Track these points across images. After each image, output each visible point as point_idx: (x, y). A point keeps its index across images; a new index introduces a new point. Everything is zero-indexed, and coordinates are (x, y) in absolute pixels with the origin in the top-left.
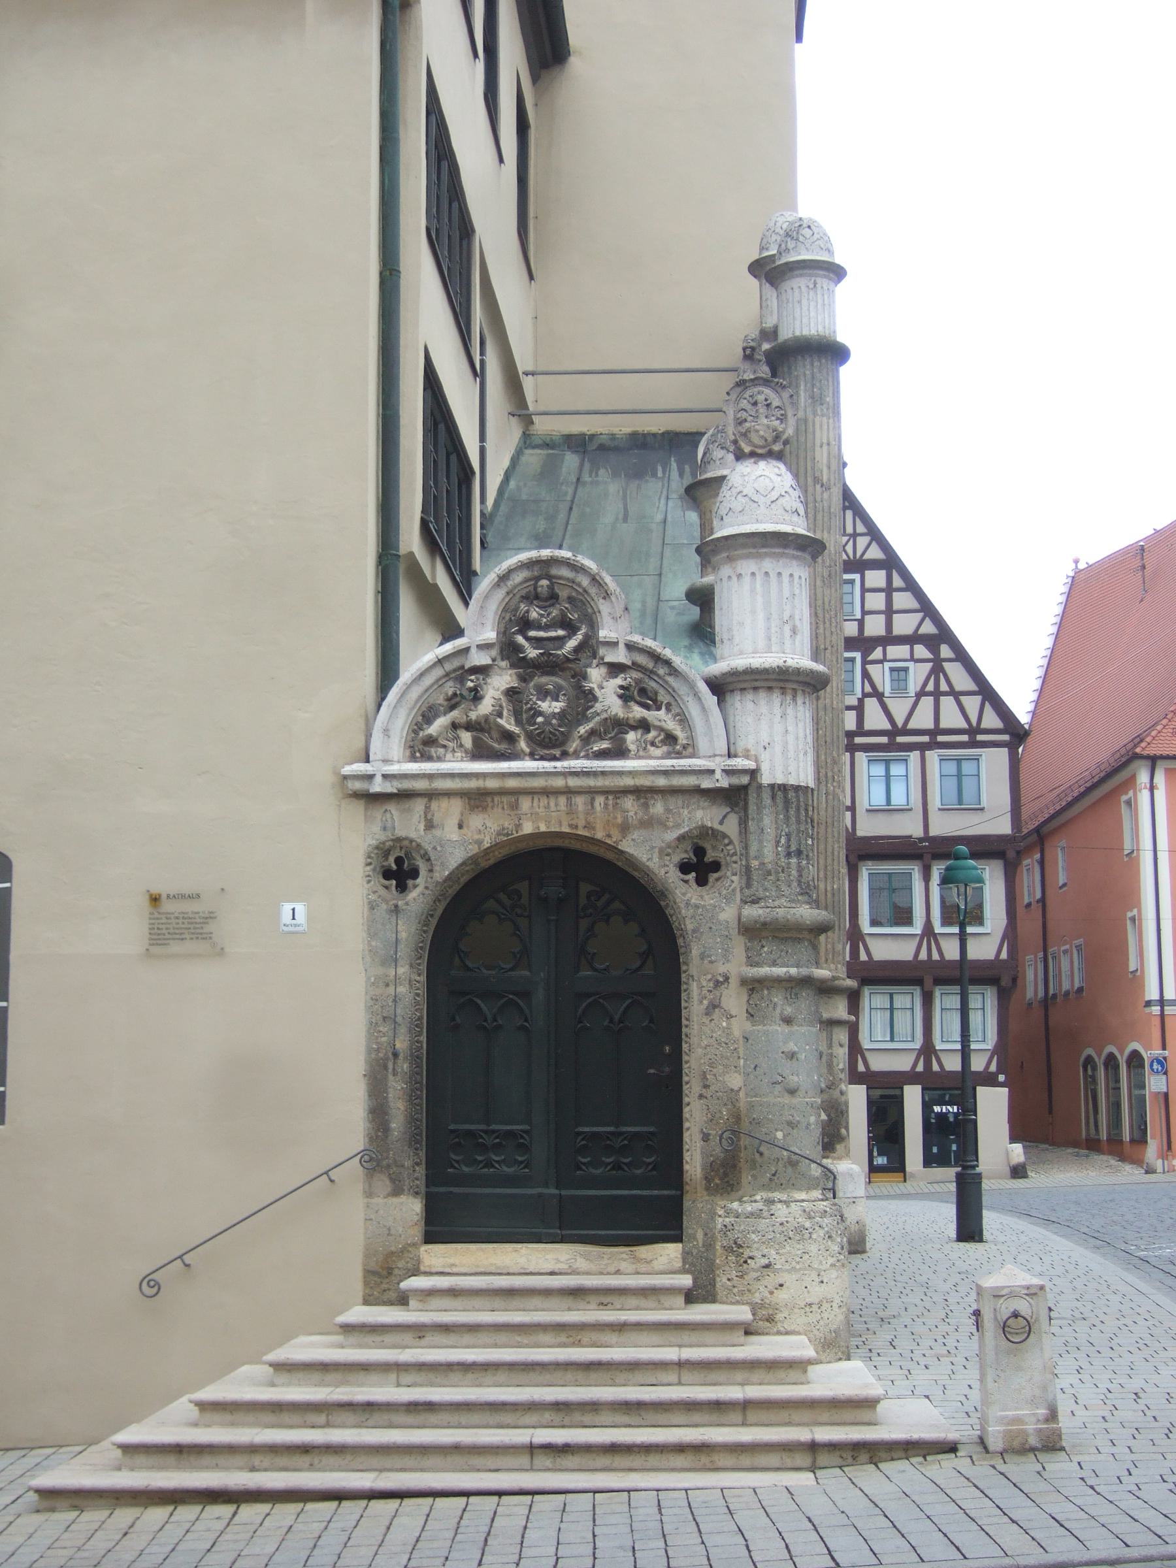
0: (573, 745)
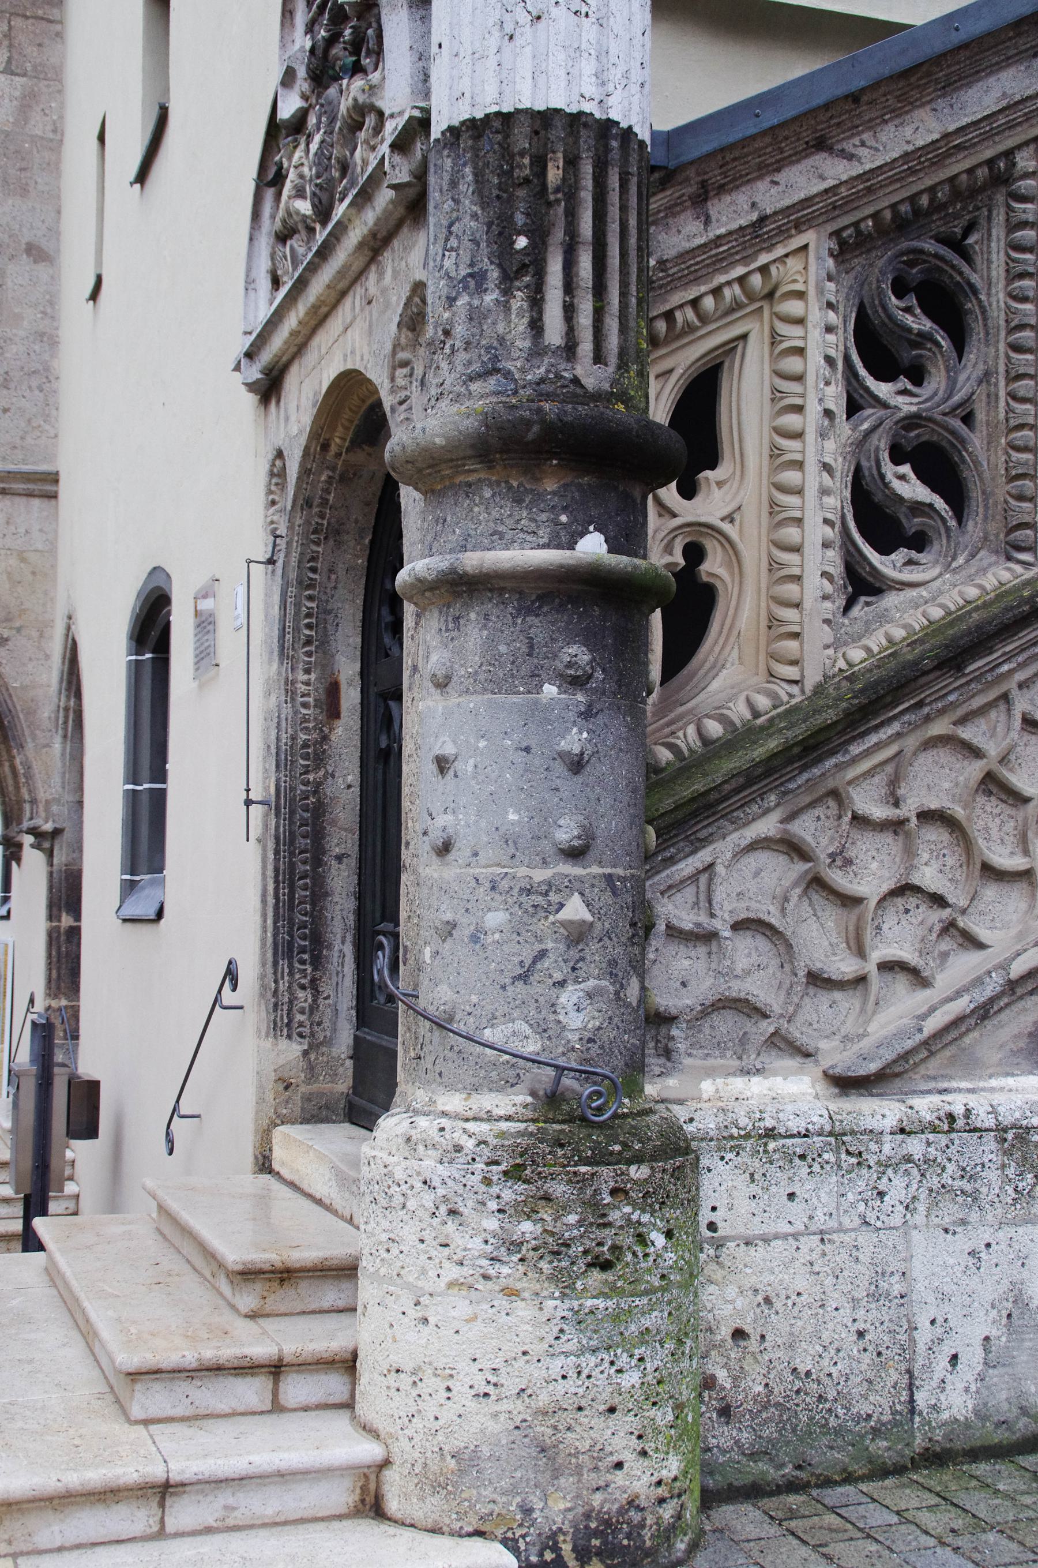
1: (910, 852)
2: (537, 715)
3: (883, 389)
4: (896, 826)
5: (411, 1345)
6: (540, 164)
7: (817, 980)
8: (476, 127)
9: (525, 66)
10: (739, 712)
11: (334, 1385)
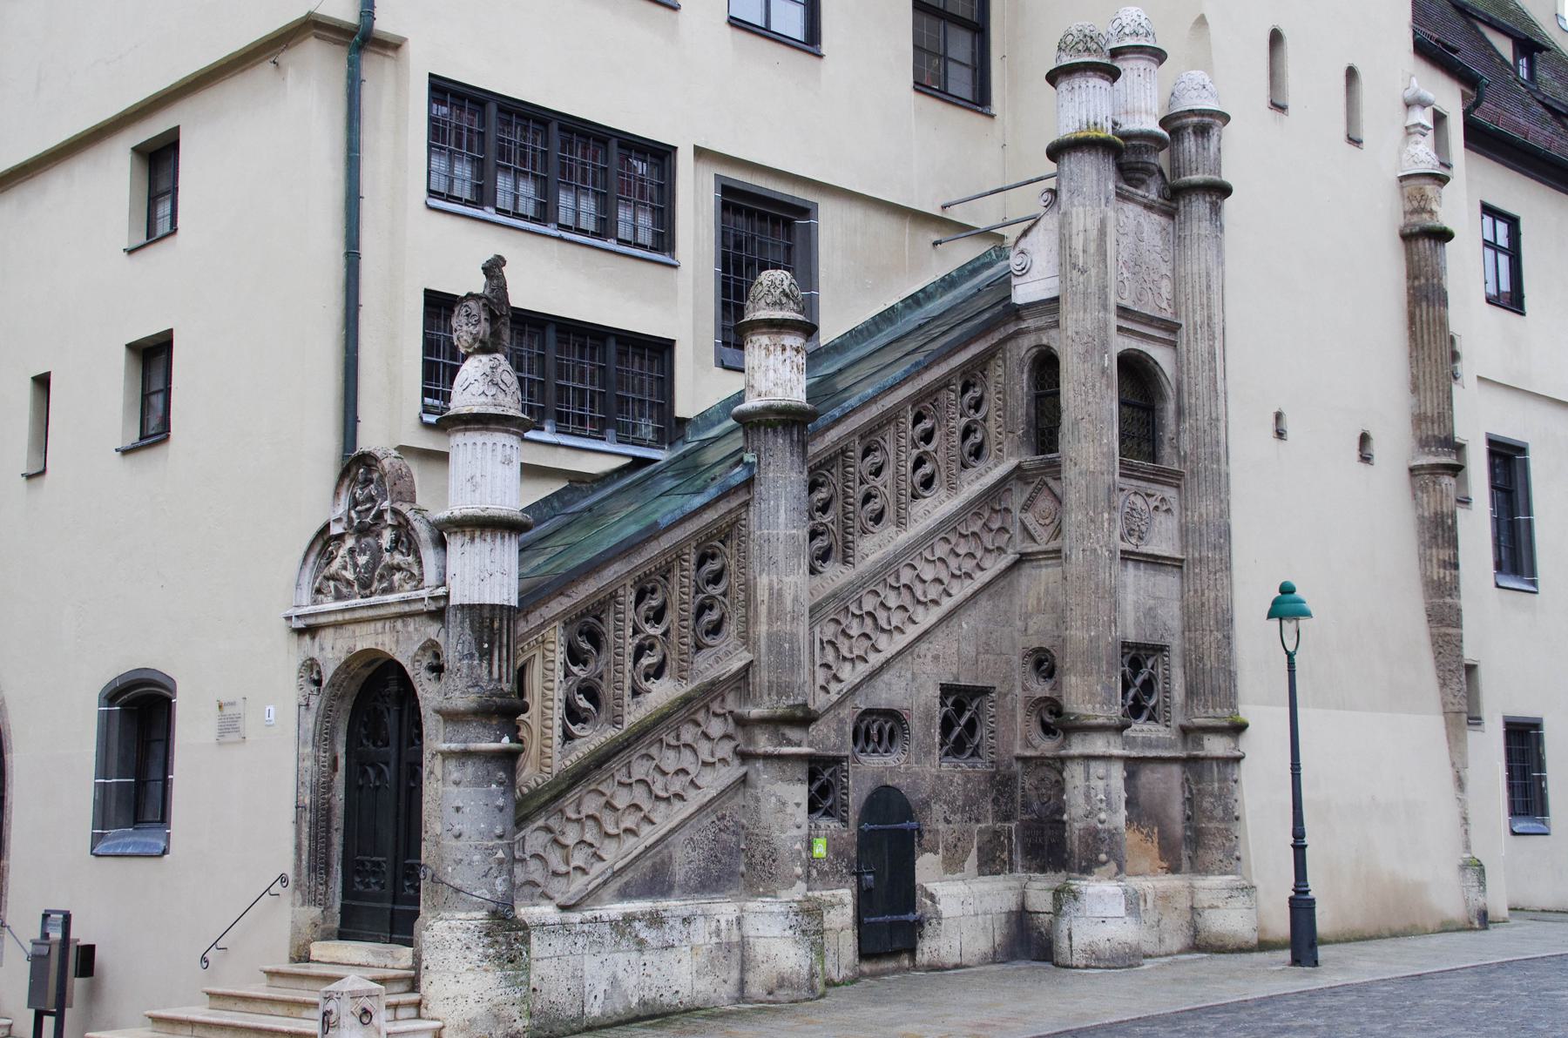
0: (376, 584)
1: (583, 829)
2: (490, 794)
3: (575, 669)
4: (578, 821)
5: (453, 989)
6: (492, 622)
7: (555, 874)
8: (471, 607)
9: (487, 590)
10: (533, 784)
11: (412, 1012)
